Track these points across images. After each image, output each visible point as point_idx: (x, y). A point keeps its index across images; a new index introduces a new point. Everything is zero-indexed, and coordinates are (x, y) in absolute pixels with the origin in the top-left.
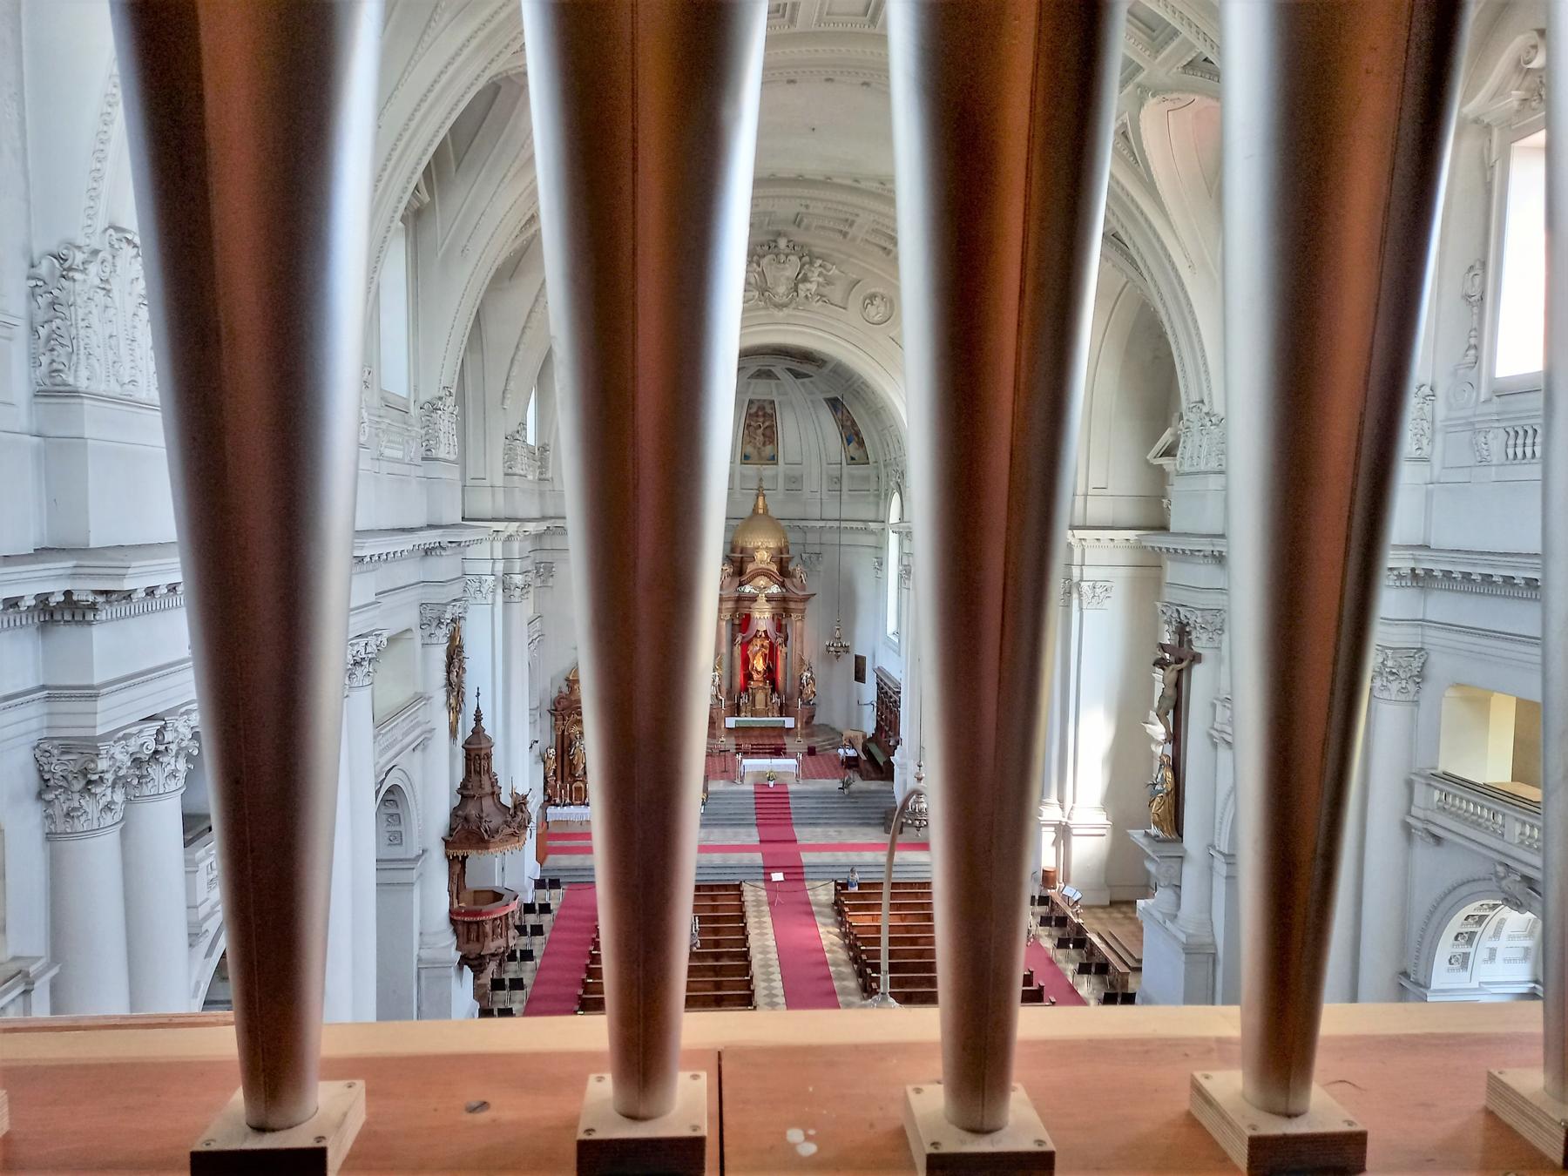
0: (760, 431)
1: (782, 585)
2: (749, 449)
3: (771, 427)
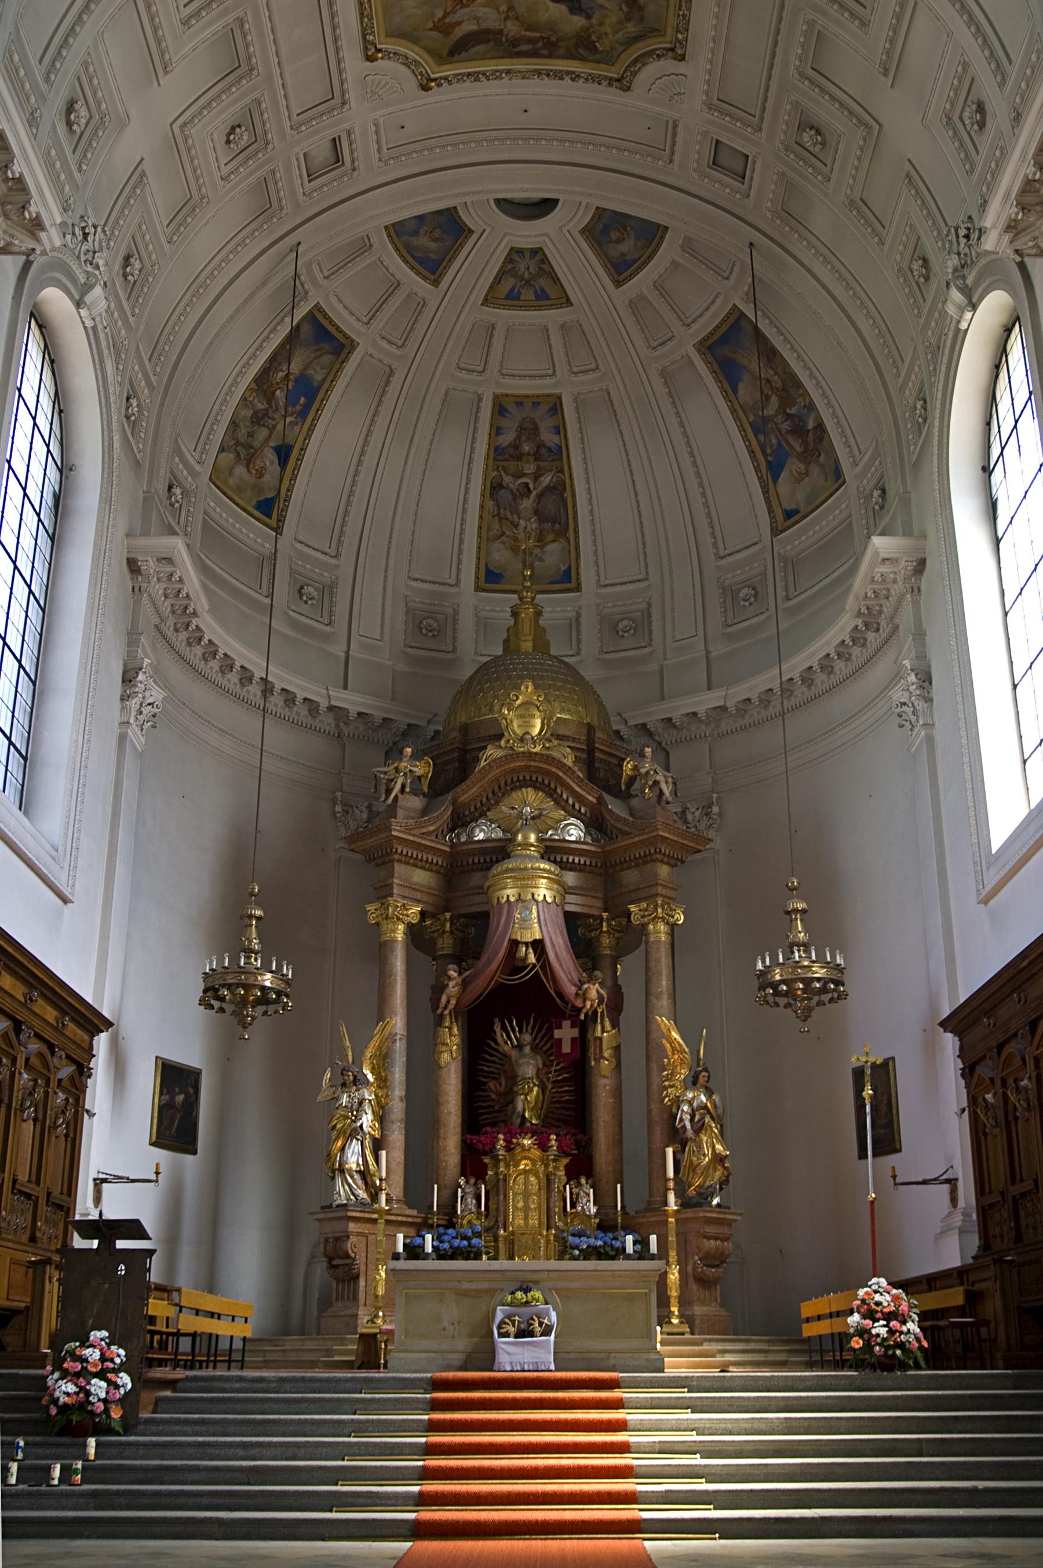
0: (527, 504)
1: (595, 823)
2: (500, 555)
3: (561, 490)
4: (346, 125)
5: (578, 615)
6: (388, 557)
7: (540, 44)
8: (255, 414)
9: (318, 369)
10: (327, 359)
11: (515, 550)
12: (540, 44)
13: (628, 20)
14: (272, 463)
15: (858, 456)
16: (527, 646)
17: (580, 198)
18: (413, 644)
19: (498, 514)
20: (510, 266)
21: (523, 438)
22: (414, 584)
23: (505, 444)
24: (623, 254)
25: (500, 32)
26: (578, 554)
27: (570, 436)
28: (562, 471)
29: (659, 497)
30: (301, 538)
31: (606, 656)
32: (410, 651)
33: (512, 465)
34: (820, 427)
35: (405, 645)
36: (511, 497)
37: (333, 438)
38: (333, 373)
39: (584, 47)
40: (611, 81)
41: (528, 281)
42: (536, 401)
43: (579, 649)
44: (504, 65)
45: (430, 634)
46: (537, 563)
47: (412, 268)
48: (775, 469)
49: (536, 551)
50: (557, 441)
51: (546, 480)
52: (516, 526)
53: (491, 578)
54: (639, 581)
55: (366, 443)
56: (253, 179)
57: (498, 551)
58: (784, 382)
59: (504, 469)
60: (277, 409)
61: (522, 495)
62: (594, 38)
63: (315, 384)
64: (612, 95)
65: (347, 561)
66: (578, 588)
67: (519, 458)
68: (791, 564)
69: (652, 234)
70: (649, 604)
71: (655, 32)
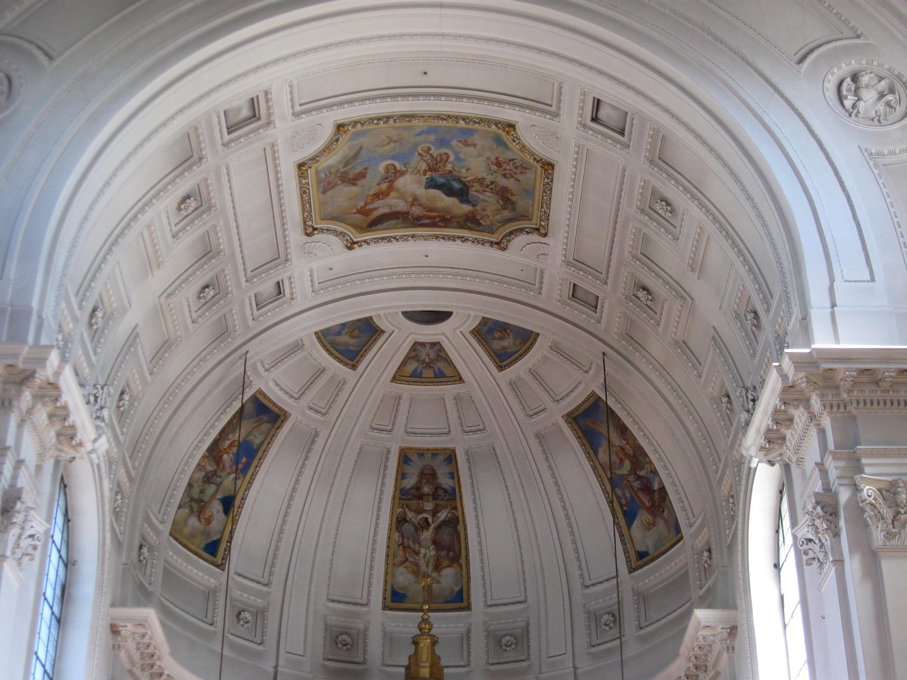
0: (427, 535)
2: (404, 578)
3: (455, 524)
4: (288, 274)
5: (469, 631)
6: (310, 583)
7: (438, 219)
8: (205, 476)
9: (257, 434)
10: (265, 427)
11: (416, 572)
12: (438, 219)
13: (504, 209)
14: (218, 512)
15: (692, 520)
16: (425, 672)
17: (467, 312)
18: (331, 657)
19: (402, 544)
20: (414, 354)
21: (424, 481)
22: (331, 605)
23: (409, 487)
24: (504, 348)
25: (408, 213)
26: (469, 578)
28: (455, 508)
29: (536, 534)
30: (240, 571)
31: (492, 668)
32: (328, 663)
33: (414, 503)
34: (662, 489)
35: (324, 659)
36: (412, 529)
37: (268, 491)
38: (270, 438)
39: (471, 222)
40: (492, 244)
41: (428, 366)
42: (435, 453)
43: (469, 661)
44: (410, 232)
45: (345, 648)
46: (434, 585)
47: (336, 358)
48: (630, 517)
49: (435, 575)
50: (452, 485)
51: (443, 515)
52: (417, 554)
53: (396, 598)
54: (520, 602)
55: (294, 490)
56: (215, 318)
57: (402, 574)
58: (634, 451)
59: (407, 506)
60: (224, 469)
61: (423, 528)
62: (478, 217)
63: (255, 447)
64: (494, 252)
65: (276, 589)
66: (468, 608)
67: (420, 497)
68: (642, 598)
69: (527, 339)
70: (528, 624)
71: (525, 217)
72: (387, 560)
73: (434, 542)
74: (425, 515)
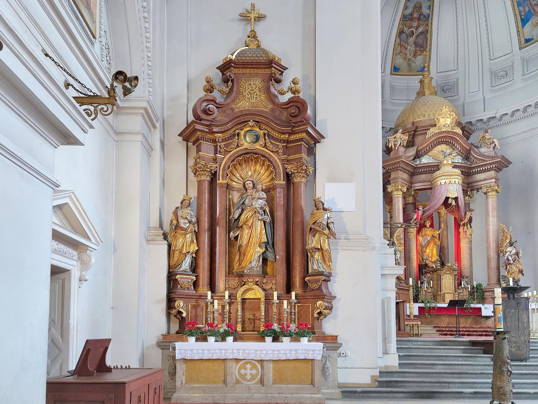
0: (412, 39)
3: (426, 34)
27: (434, 10)
51: (420, 29)
72: (393, 51)
73: (415, 43)
74: (412, 29)
